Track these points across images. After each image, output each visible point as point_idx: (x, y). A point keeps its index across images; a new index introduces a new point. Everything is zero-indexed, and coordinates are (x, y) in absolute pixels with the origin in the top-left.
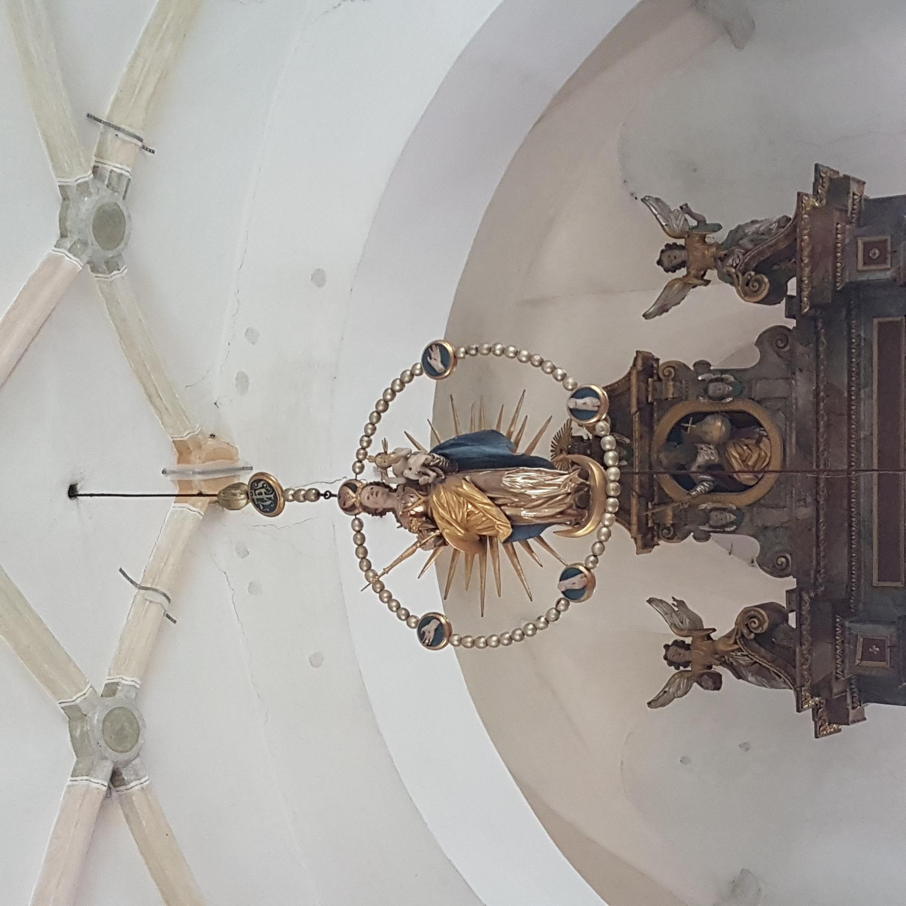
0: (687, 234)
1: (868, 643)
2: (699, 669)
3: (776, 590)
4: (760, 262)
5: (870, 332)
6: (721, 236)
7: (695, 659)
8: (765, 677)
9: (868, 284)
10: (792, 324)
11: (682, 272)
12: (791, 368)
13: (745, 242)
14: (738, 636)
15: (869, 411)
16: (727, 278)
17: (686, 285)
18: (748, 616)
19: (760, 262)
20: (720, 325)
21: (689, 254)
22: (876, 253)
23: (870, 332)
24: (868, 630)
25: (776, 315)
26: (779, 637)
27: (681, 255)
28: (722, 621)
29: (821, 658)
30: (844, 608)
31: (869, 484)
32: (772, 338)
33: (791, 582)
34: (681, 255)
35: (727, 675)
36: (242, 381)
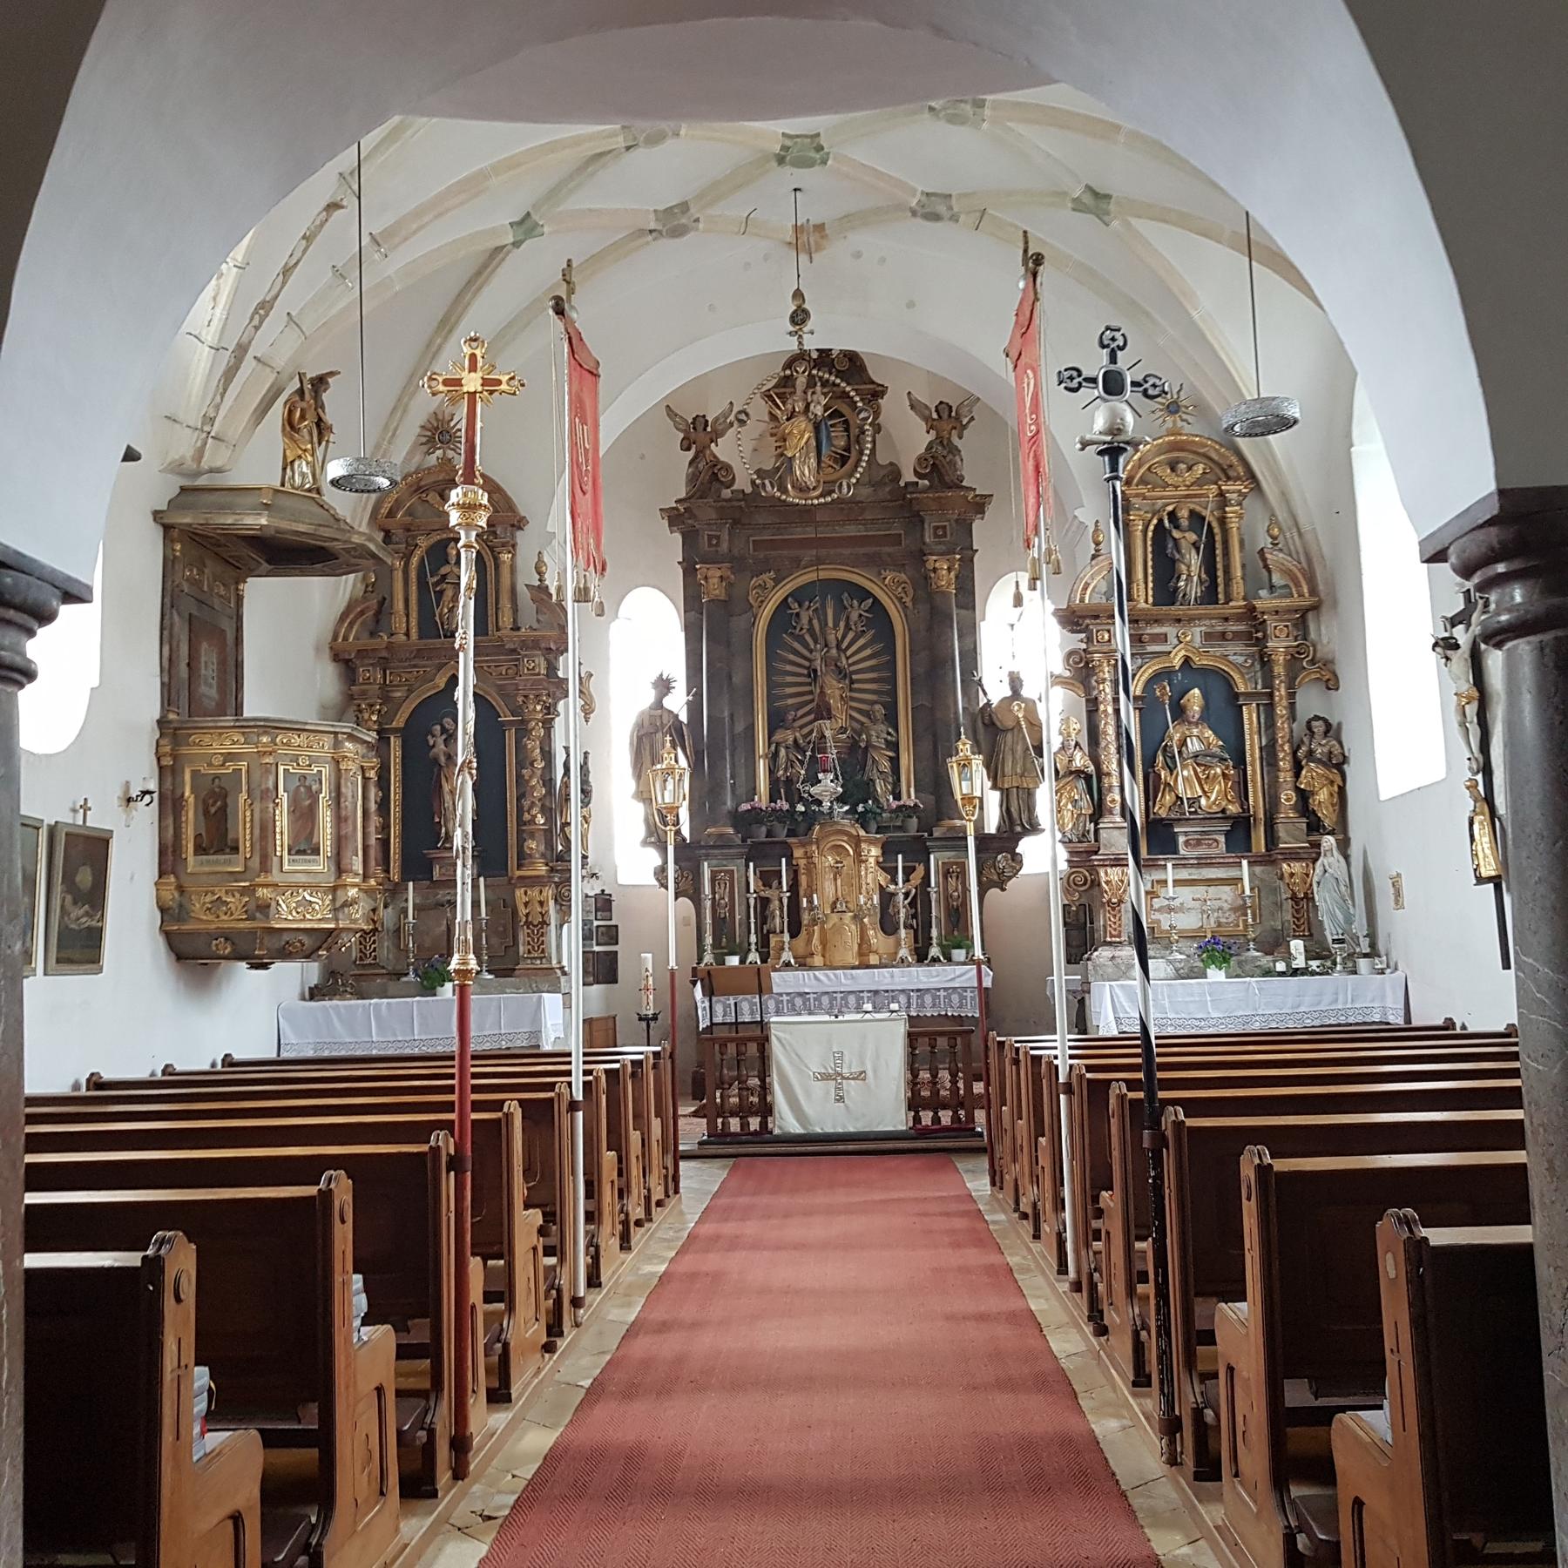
0: (958, 418)
1: (718, 537)
2: (693, 436)
3: (742, 483)
4: (939, 466)
5: (896, 529)
6: (955, 441)
7: (698, 434)
8: (692, 479)
9: (923, 529)
10: (902, 484)
11: (935, 416)
12: (876, 485)
13: (950, 457)
14: (715, 463)
15: (852, 530)
16: (929, 447)
17: (927, 419)
18: (728, 468)
19: (939, 466)
20: (905, 440)
21: (947, 419)
22: (940, 532)
23: (896, 529)
24: (725, 536)
25: (908, 476)
26: (716, 485)
27: (945, 416)
28: (723, 450)
29: (706, 512)
30: (736, 522)
31: (810, 533)
32: (894, 472)
33: (749, 490)
34: (945, 416)
35: (691, 454)
36: (858, 255)
